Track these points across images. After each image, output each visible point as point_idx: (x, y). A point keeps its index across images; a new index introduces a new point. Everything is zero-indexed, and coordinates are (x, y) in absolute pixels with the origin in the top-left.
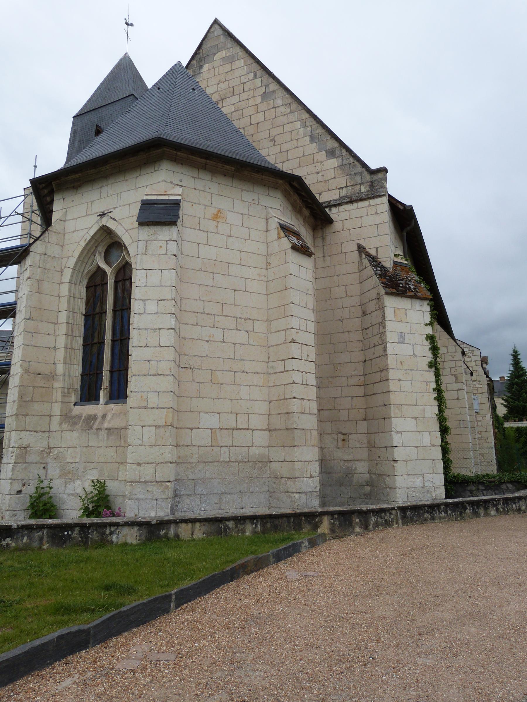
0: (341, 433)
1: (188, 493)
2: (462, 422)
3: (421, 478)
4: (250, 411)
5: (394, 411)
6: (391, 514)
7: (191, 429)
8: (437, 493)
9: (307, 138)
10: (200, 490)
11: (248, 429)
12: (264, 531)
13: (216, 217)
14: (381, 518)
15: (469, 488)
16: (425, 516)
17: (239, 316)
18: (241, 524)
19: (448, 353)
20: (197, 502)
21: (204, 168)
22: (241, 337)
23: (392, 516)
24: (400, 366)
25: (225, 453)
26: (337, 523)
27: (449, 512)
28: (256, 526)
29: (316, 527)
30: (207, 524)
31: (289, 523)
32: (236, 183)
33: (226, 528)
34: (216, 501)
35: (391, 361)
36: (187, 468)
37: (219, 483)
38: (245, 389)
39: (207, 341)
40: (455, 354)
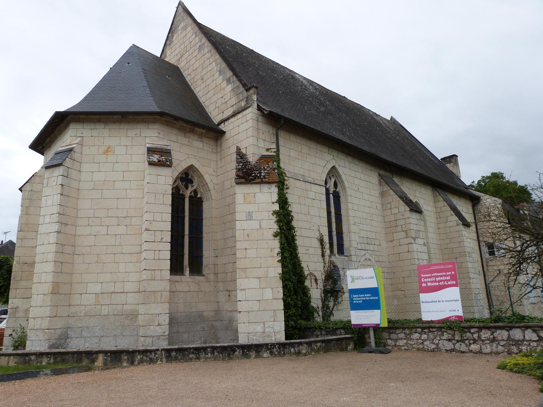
0: (227, 290)
1: (76, 336)
2: (412, 271)
3: (262, 325)
4: (125, 280)
5: (239, 273)
6: (156, 354)
7: (81, 294)
8: (276, 337)
9: (218, 73)
10: (85, 334)
11: (123, 293)
12: (55, 363)
13: (106, 152)
14: (146, 356)
15: (315, 333)
16: (191, 356)
17: (120, 215)
18: (40, 358)
19: (399, 212)
20: (83, 342)
21: (99, 121)
22: (122, 230)
23: (157, 356)
24: (247, 238)
25: (105, 309)
26: (109, 359)
27: (216, 353)
28: (50, 359)
29: (93, 361)
30: (18, 357)
31: (73, 358)
32: (123, 126)
33: (30, 360)
34: (97, 341)
35: (239, 235)
36: (77, 320)
37: (99, 330)
38: (122, 265)
39: (95, 235)
40: (404, 213)
